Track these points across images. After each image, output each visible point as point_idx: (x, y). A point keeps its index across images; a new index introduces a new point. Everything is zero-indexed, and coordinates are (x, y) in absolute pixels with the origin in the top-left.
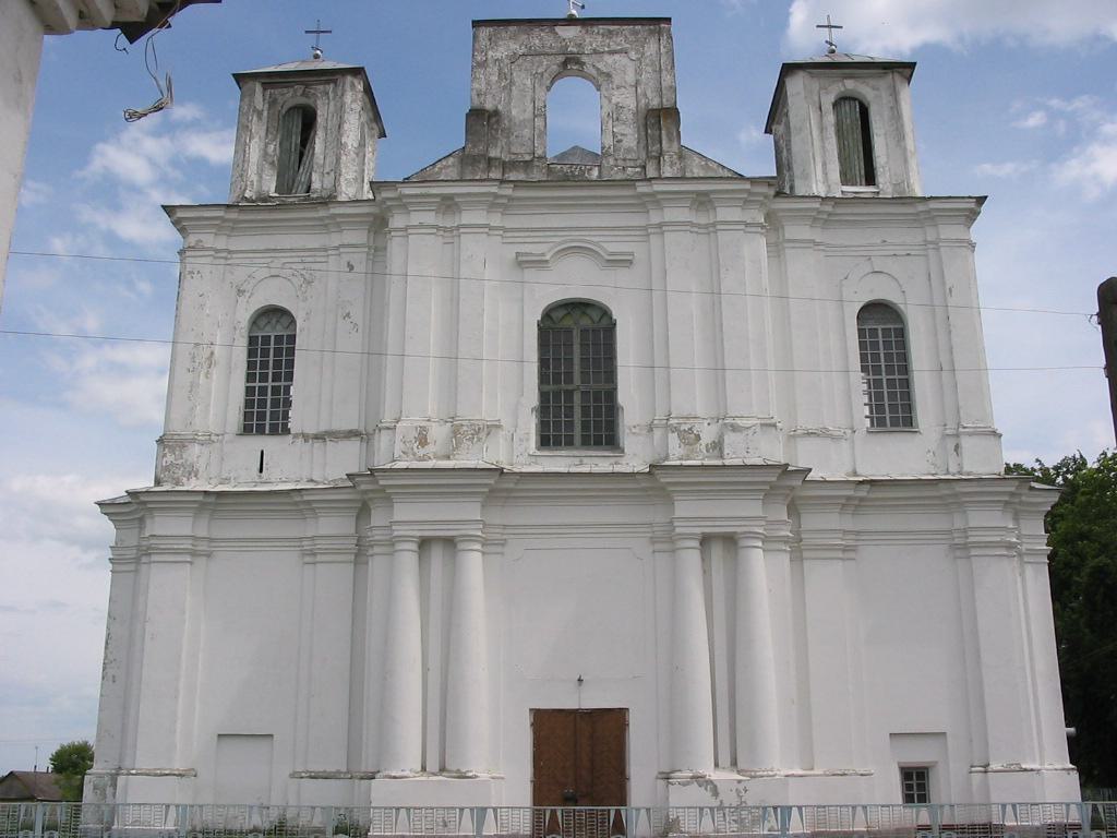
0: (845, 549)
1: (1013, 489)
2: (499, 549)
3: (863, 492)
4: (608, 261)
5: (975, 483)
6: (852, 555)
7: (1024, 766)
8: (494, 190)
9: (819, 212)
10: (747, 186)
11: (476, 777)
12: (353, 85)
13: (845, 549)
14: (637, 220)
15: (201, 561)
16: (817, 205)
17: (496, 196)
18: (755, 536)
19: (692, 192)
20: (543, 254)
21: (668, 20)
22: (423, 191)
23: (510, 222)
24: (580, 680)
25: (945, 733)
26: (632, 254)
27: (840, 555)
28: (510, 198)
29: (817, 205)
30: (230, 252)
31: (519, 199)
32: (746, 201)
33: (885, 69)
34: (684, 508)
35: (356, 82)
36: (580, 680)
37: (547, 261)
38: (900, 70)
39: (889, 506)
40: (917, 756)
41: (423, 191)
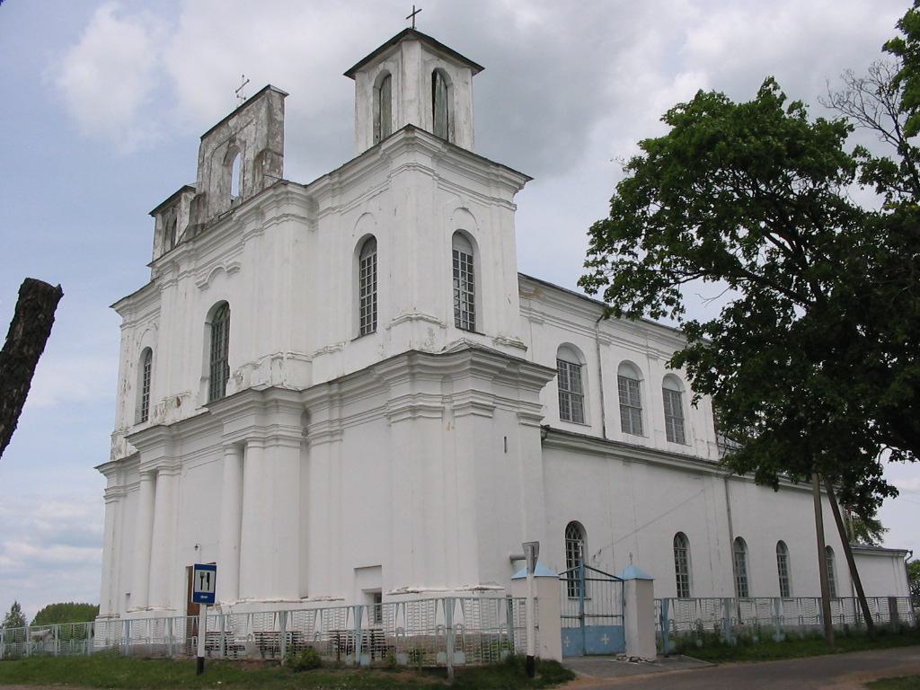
0: (332, 434)
1: (405, 363)
2: (178, 471)
3: (335, 389)
4: (228, 272)
5: (383, 366)
6: (338, 437)
7: (409, 590)
8: (184, 249)
9: (333, 185)
10: (271, 192)
11: (151, 609)
12: (186, 197)
13: (332, 434)
14: (237, 241)
15: (121, 499)
16: (327, 182)
17: (189, 251)
18: (253, 439)
19: (252, 209)
20: (204, 280)
21: (269, 86)
22: (163, 262)
23: (201, 263)
24: (197, 547)
25: (380, 566)
26: (235, 263)
27: (328, 439)
28: (196, 250)
29: (327, 182)
30: (135, 322)
31: (199, 248)
32: (278, 202)
33: (394, 43)
34: (228, 429)
35: (188, 195)
36: (197, 547)
37: (207, 284)
38: (404, 38)
39: (369, 391)
40: (372, 583)
41: (163, 262)
